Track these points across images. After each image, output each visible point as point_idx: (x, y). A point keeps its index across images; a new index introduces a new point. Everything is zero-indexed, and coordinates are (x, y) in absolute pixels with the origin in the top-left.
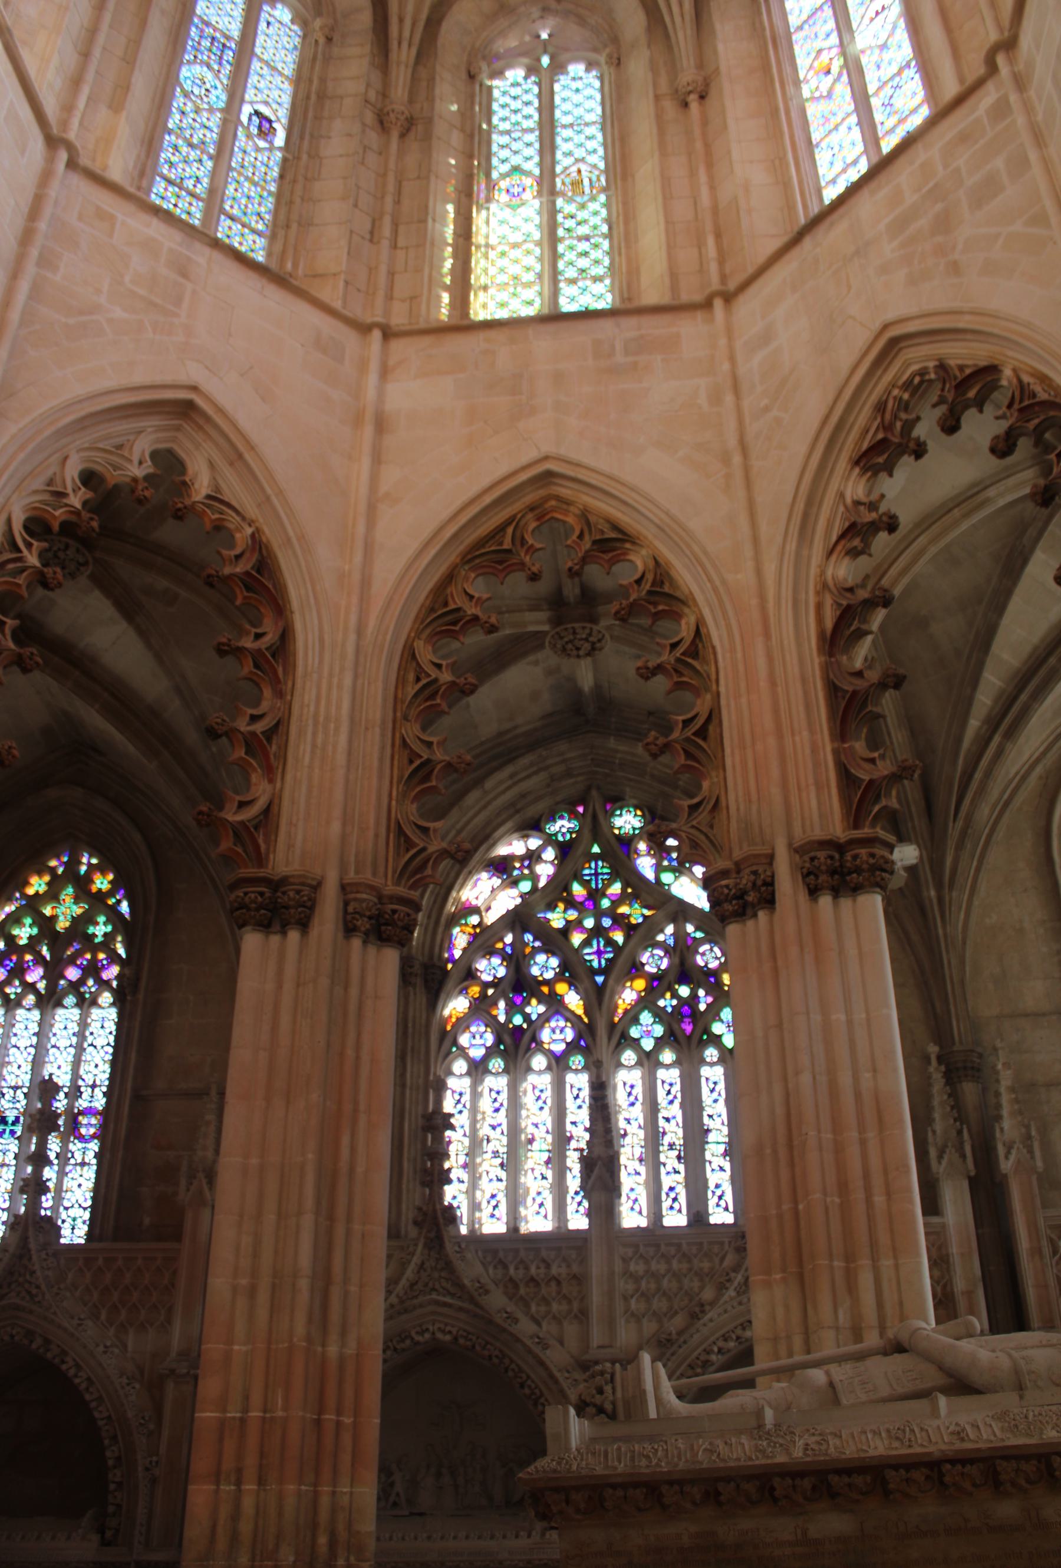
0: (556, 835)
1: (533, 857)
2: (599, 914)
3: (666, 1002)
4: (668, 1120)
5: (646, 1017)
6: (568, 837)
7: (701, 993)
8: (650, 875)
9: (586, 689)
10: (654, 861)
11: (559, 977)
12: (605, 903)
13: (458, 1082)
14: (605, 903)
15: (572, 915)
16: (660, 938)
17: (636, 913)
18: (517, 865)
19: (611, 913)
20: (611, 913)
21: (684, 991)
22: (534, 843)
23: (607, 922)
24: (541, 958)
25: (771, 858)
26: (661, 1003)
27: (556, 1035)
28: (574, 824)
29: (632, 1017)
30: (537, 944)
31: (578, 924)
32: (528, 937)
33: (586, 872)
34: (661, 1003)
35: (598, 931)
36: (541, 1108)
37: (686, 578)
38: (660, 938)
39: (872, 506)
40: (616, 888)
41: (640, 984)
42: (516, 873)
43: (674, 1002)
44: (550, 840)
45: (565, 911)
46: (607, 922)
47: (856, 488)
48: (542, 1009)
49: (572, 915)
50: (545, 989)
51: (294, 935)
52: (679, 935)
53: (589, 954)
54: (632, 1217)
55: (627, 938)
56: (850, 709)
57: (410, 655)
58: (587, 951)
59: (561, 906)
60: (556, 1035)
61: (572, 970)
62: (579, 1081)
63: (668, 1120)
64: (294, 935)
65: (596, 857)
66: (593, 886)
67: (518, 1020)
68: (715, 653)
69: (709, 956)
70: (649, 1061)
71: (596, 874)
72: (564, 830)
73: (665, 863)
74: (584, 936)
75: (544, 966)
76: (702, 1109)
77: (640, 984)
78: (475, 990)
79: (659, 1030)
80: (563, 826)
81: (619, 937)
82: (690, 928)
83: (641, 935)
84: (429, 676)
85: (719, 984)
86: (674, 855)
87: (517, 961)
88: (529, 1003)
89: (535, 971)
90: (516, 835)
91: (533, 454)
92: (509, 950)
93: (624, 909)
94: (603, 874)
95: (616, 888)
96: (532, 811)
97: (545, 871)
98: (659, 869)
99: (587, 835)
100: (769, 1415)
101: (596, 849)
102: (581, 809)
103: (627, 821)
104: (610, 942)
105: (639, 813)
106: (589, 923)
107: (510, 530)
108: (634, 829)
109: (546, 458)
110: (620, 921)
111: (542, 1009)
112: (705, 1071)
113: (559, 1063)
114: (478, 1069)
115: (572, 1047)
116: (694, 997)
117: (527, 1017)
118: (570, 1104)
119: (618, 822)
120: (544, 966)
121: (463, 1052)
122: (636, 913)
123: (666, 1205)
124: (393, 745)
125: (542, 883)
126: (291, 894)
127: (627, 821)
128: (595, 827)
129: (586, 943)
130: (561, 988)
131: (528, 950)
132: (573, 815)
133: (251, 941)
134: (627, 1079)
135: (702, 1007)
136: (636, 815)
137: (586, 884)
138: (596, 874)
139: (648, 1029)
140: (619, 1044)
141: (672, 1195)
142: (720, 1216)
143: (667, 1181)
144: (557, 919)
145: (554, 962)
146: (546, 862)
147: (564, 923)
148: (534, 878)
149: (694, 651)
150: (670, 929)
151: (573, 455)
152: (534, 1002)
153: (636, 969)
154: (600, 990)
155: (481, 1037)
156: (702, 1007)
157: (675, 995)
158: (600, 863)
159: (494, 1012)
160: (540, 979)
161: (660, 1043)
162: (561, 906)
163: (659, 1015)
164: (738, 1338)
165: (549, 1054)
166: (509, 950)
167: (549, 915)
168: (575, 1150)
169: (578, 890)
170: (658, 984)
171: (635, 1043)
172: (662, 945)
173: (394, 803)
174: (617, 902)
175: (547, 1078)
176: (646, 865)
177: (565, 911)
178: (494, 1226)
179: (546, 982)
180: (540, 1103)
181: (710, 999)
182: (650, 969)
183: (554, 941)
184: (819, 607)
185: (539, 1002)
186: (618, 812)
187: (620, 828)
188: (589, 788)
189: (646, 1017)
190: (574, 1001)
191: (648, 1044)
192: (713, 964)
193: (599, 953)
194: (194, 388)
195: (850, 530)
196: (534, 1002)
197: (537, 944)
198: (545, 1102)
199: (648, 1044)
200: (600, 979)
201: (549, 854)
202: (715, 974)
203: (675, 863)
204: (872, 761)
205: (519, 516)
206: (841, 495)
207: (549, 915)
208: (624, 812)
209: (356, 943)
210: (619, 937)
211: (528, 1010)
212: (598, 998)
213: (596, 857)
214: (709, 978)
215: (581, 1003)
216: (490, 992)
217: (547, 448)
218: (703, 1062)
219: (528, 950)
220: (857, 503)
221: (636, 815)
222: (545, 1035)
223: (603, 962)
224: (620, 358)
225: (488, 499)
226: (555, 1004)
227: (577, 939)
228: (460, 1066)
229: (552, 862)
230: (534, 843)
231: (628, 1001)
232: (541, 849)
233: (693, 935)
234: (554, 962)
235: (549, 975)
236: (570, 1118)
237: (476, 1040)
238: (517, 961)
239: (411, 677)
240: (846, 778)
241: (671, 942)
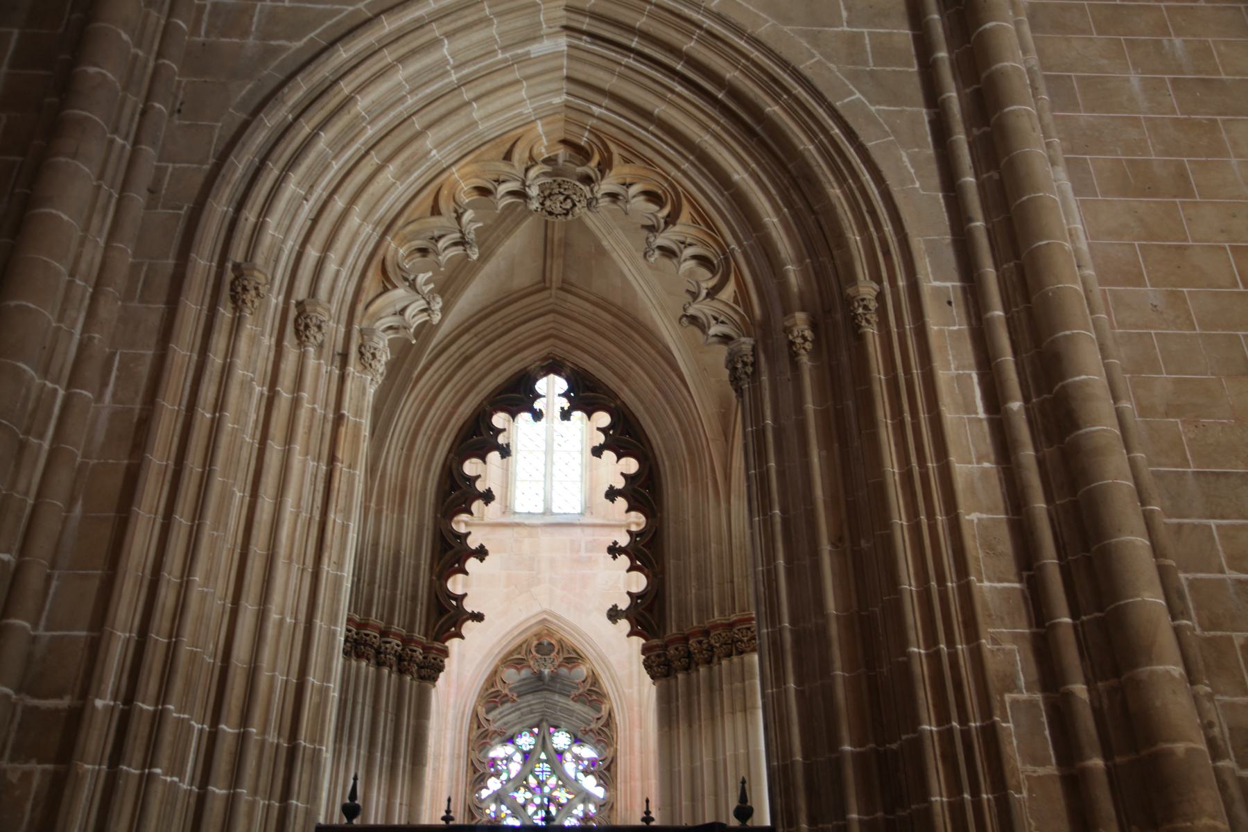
12: (546, 790)
15: (529, 795)
16: (575, 812)
32: (503, 808)
37: (606, 684)
44: (519, 749)
59: (522, 789)
91: (536, 609)
93: (555, 793)
96: (509, 733)
97: (515, 768)
99: (539, 748)
106: (537, 800)
107: (525, 646)
128: (543, 743)
129: (536, 813)
144: (521, 796)
148: (509, 771)
149: (607, 725)
151: (558, 612)
167: (515, 794)
169: (532, 782)
188: (541, 721)
207: (515, 794)
213: (543, 761)
217: (546, 606)
224: (583, 554)
227: (531, 810)
239: (475, 726)
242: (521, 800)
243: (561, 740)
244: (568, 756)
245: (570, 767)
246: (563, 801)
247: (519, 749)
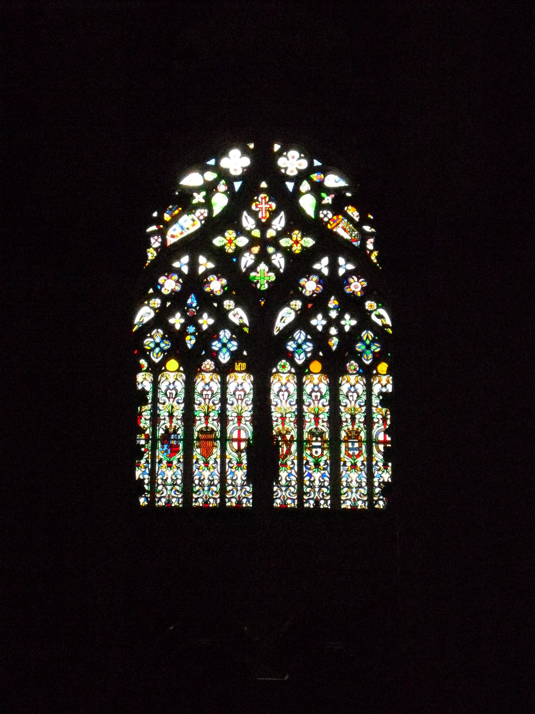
1: (210, 188)
22: (210, 176)
27: (225, 345)
54: (284, 495)
60: (225, 345)
65: (263, 191)
80: (236, 162)
83: (300, 264)
97: (220, 201)
102: (252, 146)
132: (245, 152)
139: (301, 344)
154: (262, 310)
176: (308, 203)
201: (222, 187)
226: (222, 319)
230: (210, 176)
243: (292, 162)
246: (297, 249)
247: (223, 174)
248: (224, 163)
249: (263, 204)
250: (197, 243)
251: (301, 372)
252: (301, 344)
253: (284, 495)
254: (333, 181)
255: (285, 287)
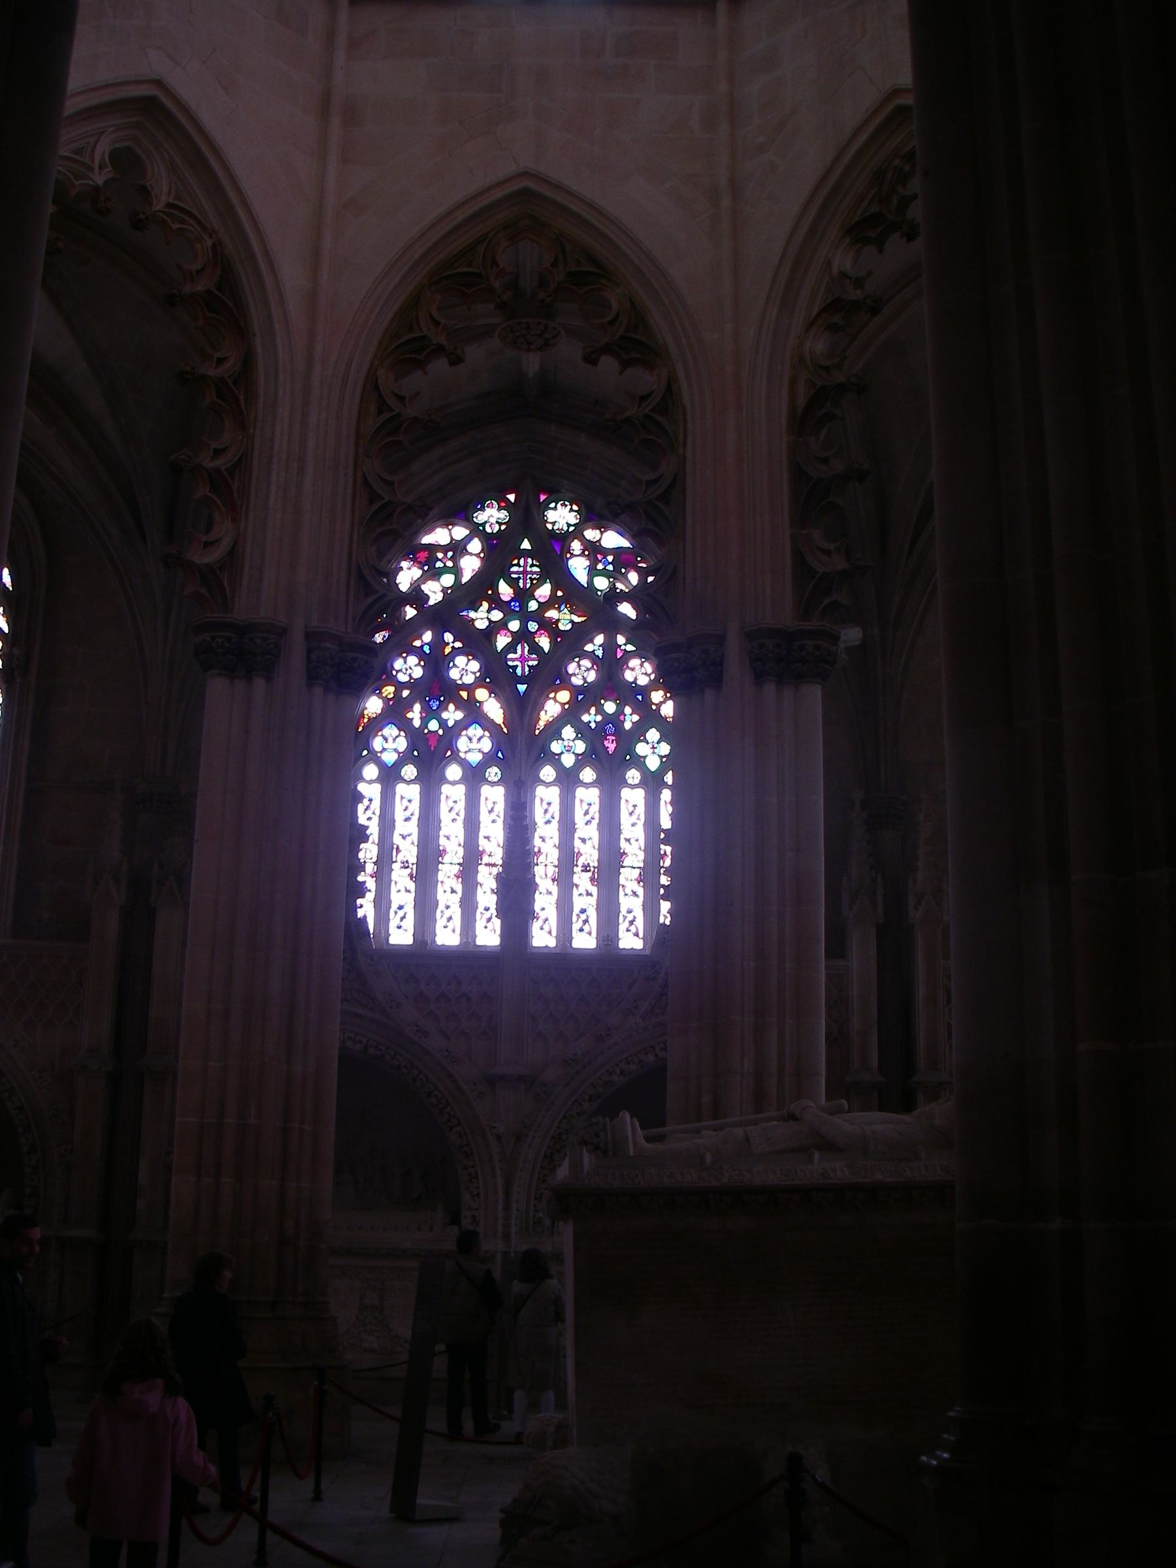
0: (483, 525)
1: (458, 549)
2: (525, 617)
3: (591, 718)
4: (583, 841)
5: (568, 732)
6: (496, 528)
7: (628, 710)
8: (582, 578)
9: (531, 374)
10: (588, 563)
11: (480, 682)
12: (533, 606)
13: (370, 790)
14: (533, 606)
15: (497, 615)
16: (589, 648)
17: (565, 619)
18: (440, 555)
19: (538, 616)
20: (538, 616)
21: (610, 707)
23: (533, 626)
24: (461, 660)
25: (722, 639)
26: (585, 718)
27: (474, 745)
28: (503, 515)
29: (553, 731)
30: (458, 645)
31: (502, 626)
32: (448, 637)
33: (515, 569)
34: (585, 718)
35: (523, 636)
36: (454, 820)
38: (589, 648)
39: (859, 283)
40: (544, 591)
41: (564, 696)
42: (439, 564)
43: (599, 718)
44: (477, 530)
45: (489, 611)
46: (533, 626)
47: (843, 261)
48: (459, 715)
49: (497, 615)
50: (464, 694)
51: (259, 683)
52: (610, 646)
53: (513, 658)
55: (553, 643)
56: (812, 496)
57: (372, 385)
58: (511, 656)
59: (485, 605)
60: (474, 745)
61: (496, 674)
62: (494, 796)
63: (583, 841)
64: (259, 683)
65: (526, 554)
66: (521, 585)
67: (433, 725)
68: (685, 414)
69: (638, 671)
70: (568, 780)
71: (525, 572)
72: (493, 520)
73: (600, 566)
74: (510, 640)
75: (464, 670)
76: (620, 832)
77: (564, 696)
78: (389, 690)
79: (580, 747)
80: (492, 516)
81: (544, 642)
82: (621, 640)
83: (569, 644)
84: (392, 410)
85: (647, 701)
86: (610, 558)
87: (436, 662)
88: (446, 709)
89: (454, 674)
90: (440, 523)
92: (426, 649)
93: (552, 614)
94: (532, 573)
95: (544, 591)
97: (470, 565)
98: (592, 572)
100: (708, 1158)
101: (526, 545)
102: (512, 497)
103: (561, 516)
104: (535, 649)
105: (575, 508)
106: (514, 625)
108: (569, 525)
109: (525, 174)
110: (549, 627)
111: (459, 715)
112: (625, 793)
113: (474, 777)
114: (390, 776)
115: (490, 759)
116: (620, 712)
117: (443, 723)
118: (484, 817)
119: (551, 515)
120: (464, 670)
121: (375, 758)
122: (565, 619)
123: (576, 927)
124: (355, 485)
125: (466, 578)
126: (258, 641)
127: (561, 516)
128: (526, 519)
129: (511, 648)
130: (481, 694)
131: (448, 650)
132: (504, 505)
133: (217, 687)
134: (547, 796)
135: (628, 725)
136: (571, 510)
137: (513, 583)
138: (525, 572)
139: (569, 746)
140: (538, 758)
141: (583, 917)
142: (630, 941)
143: (578, 902)
144: (481, 617)
145: (475, 666)
146: (471, 554)
147: (487, 623)
148: (457, 571)
150: (599, 639)
152: (451, 707)
153: (561, 680)
155: (394, 740)
156: (628, 725)
157: (600, 711)
158: (530, 560)
159: (409, 715)
160: (459, 682)
161: (582, 761)
162: (485, 605)
163: (583, 731)
164: (640, 1061)
165: (464, 764)
166: (426, 649)
167: (472, 614)
168: (486, 865)
169: (505, 591)
170: (585, 697)
171: (555, 760)
172: (591, 655)
173: (355, 546)
174: (544, 607)
175: (461, 789)
177: (489, 611)
178: (401, 935)
179: (465, 687)
180: (453, 815)
181: (636, 718)
182: (577, 681)
183: (478, 643)
184: (793, 381)
185: (457, 708)
186: (552, 505)
187: (554, 523)
189: (568, 732)
190: (494, 709)
191: (568, 761)
192: (643, 681)
193: (523, 659)
194: (158, 83)
195: (834, 306)
196: (451, 707)
197: (458, 645)
198: (458, 814)
199: (568, 761)
200: (522, 688)
201: (475, 546)
202: (645, 691)
203: (610, 568)
204: (827, 552)
205: (491, 235)
206: (829, 264)
207: (472, 614)
208: (559, 506)
209: (318, 691)
210: (544, 642)
211: (445, 715)
212: (522, 709)
213: (526, 554)
214: (635, 696)
215: (501, 711)
216: (406, 693)
218: (624, 783)
219: (448, 650)
220: (843, 275)
221: (571, 510)
222: (462, 744)
223: (527, 669)
225: (460, 216)
226: (474, 713)
227: (502, 641)
228: (370, 771)
229: (478, 555)
230: (460, 532)
231: (550, 714)
232: (468, 539)
233: (623, 647)
234: (475, 666)
235: (469, 679)
236: (483, 832)
237: (390, 743)
238: (436, 662)
240: (802, 568)
241: (600, 653)
242: (481, 625)
244: (576, 546)
245: (579, 567)
246: (564, 626)
247: (477, 530)
248: (480, 517)
249: (526, 567)
250: (447, 616)
251: (568, 780)
252: (569, 746)
253: (542, 937)
254: (612, 539)
255: (549, 674)
